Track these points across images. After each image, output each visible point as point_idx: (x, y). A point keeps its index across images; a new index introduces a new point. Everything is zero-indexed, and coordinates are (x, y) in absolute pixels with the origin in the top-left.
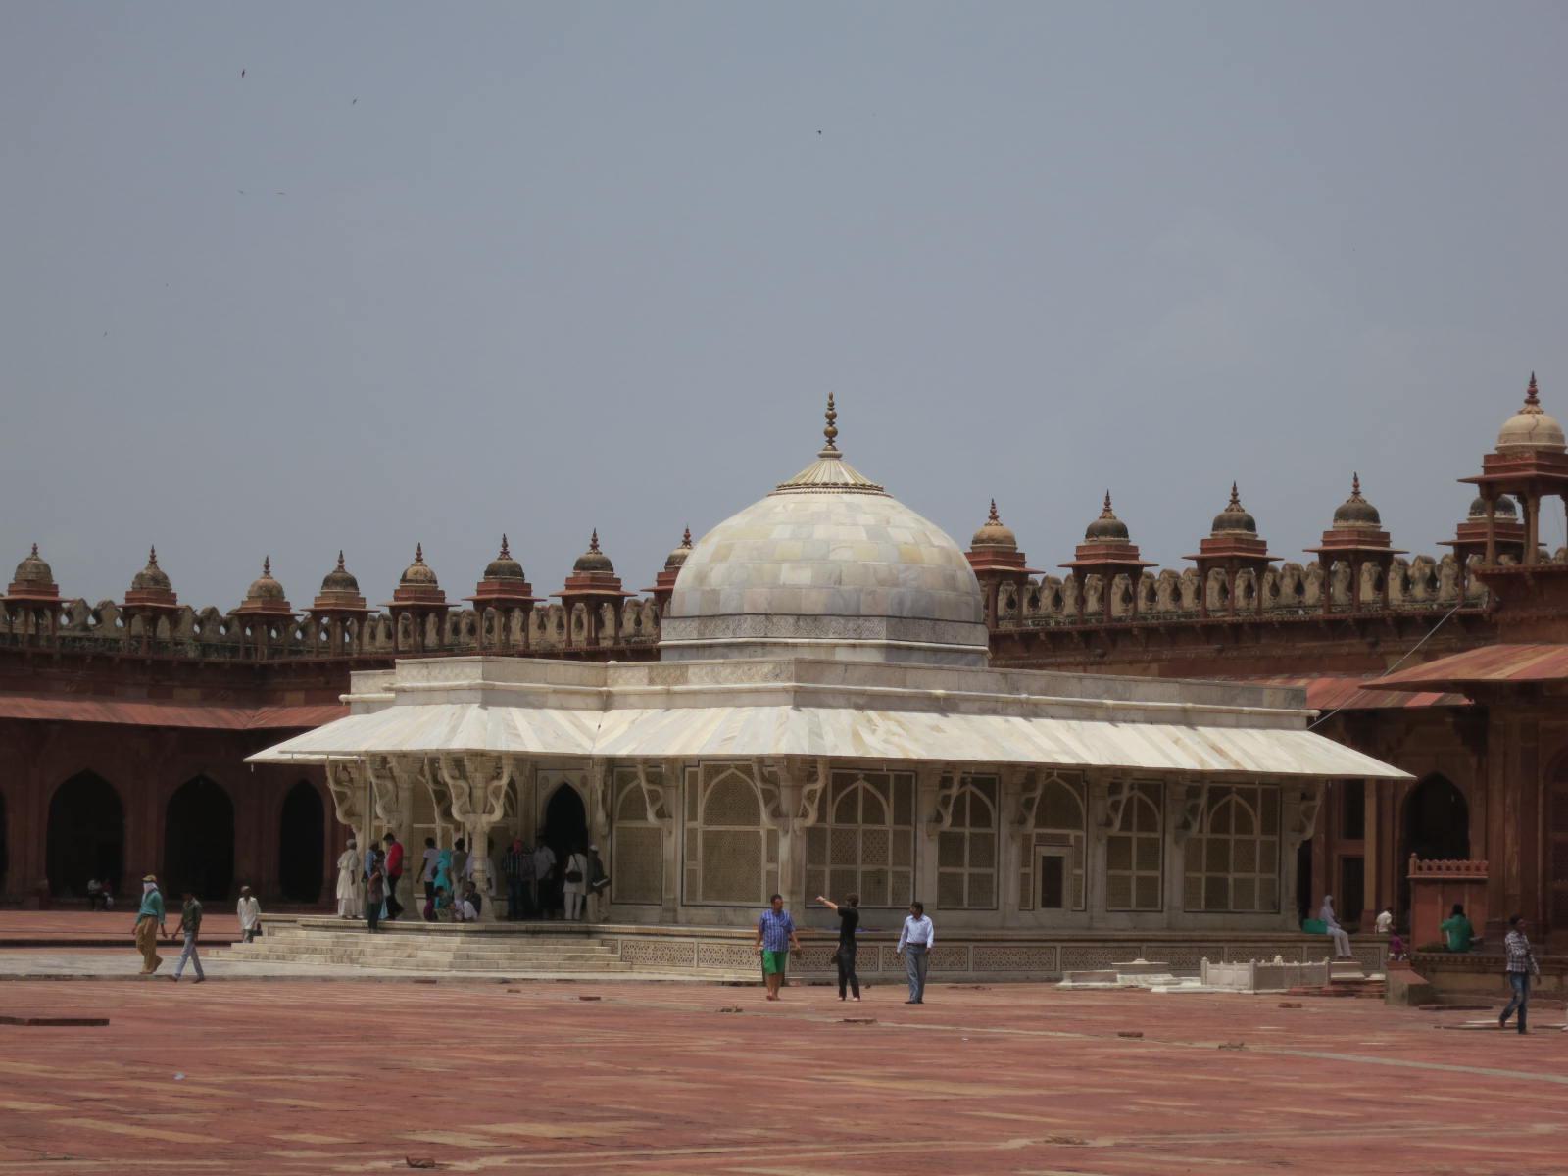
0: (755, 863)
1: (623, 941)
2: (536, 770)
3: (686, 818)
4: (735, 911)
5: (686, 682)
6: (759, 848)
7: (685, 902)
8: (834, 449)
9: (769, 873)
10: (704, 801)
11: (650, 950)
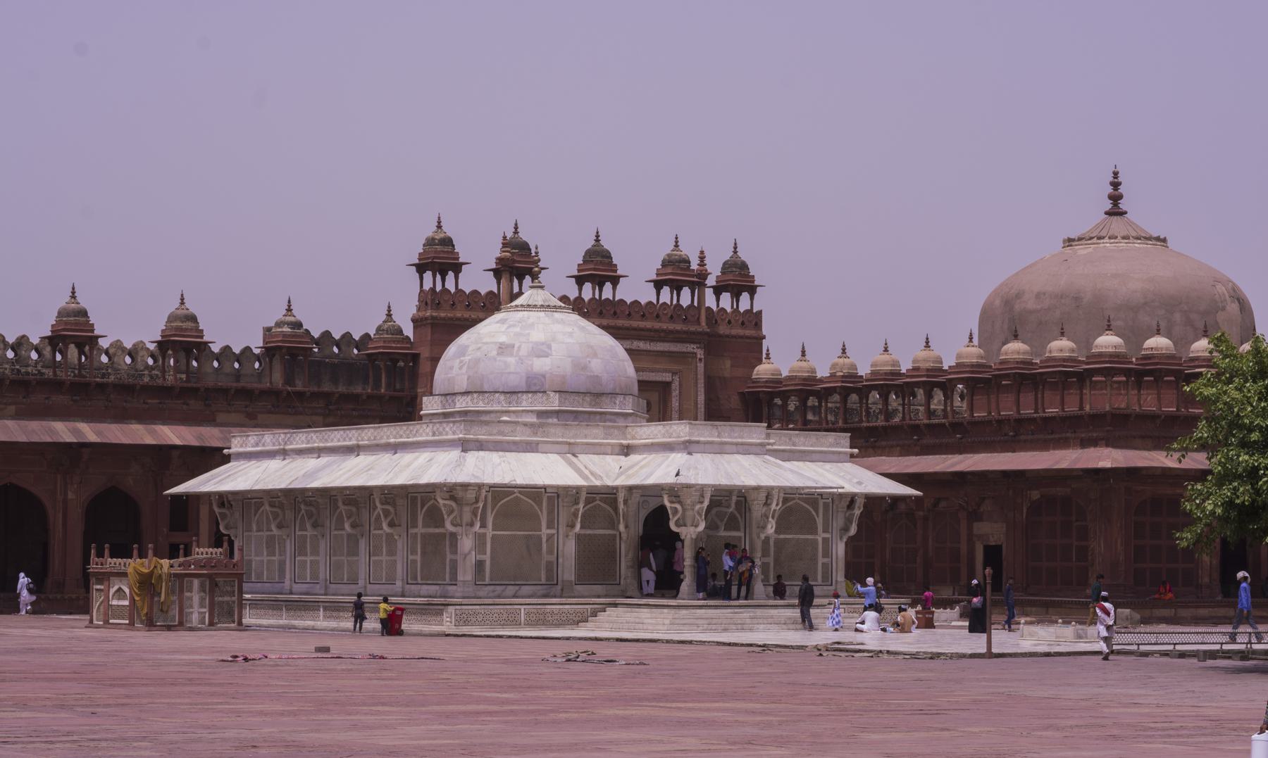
0: (814, 559)
6: (816, 549)
8: (540, 282)
9: (823, 564)
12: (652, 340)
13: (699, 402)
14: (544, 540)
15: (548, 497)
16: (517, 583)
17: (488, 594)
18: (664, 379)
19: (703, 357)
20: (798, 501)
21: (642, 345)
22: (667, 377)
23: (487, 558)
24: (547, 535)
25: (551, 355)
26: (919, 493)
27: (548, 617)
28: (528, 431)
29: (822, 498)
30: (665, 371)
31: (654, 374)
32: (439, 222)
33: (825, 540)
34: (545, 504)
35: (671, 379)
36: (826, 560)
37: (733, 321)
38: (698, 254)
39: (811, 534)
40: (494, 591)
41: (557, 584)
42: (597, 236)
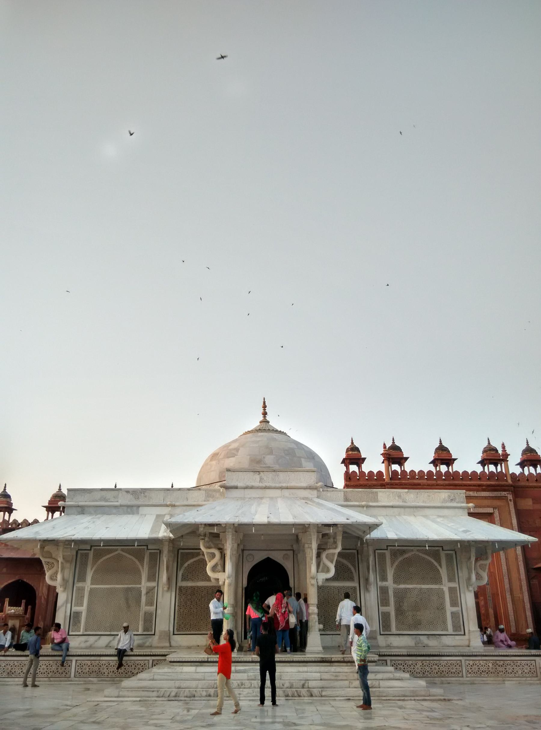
0: (441, 608)
1: (391, 660)
2: (243, 550)
3: (378, 580)
4: (428, 638)
5: (377, 501)
6: (443, 598)
7: (382, 633)
8: (266, 419)
9: (452, 613)
10: (392, 572)
11: (418, 666)
12: (478, 491)
13: (513, 523)
14: (144, 592)
15: (150, 553)
16: (113, 633)
17: (79, 644)
18: (488, 512)
19: (512, 498)
20: (417, 553)
21: (471, 493)
22: (490, 510)
23: (83, 609)
24: (147, 588)
25: (237, 456)
26: (534, 538)
27: (103, 669)
28: (129, 496)
29: (443, 550)
30: (488, 507)
31: (481, 509)
32: (352, 441)
33: (451, 590)
34: (146, 560)
35: (493, 511)
36: (455, 609)
37: (529, 479)
38: (501, 446)
39: (436, 583)
40: (86, 641)
41: (154, 635)
42: (441, 441)
